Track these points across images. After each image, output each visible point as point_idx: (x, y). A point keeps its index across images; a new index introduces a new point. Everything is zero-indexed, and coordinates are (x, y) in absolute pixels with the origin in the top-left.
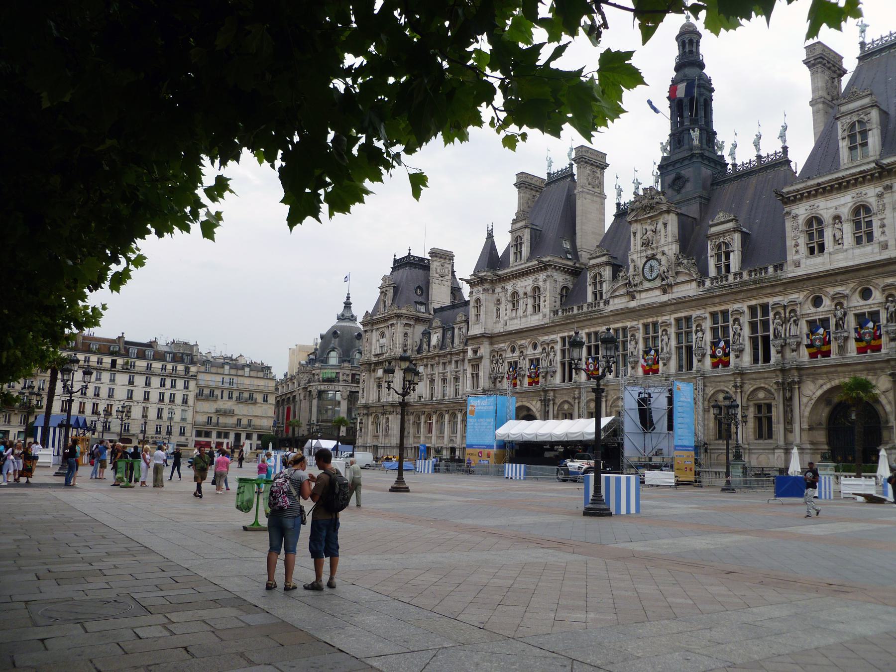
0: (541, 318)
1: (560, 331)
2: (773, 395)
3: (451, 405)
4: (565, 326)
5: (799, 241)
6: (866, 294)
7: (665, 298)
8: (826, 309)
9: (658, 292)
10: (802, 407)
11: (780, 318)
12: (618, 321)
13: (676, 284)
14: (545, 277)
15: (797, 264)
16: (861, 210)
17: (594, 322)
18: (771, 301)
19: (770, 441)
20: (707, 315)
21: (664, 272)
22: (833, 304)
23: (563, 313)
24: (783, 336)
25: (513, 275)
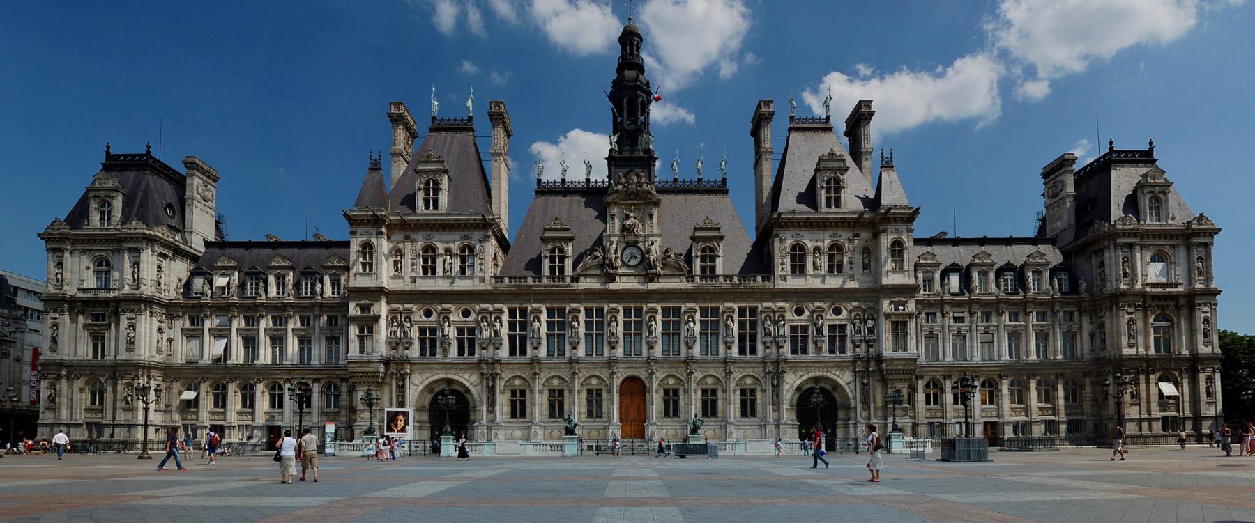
2: (760, 381)
5: (785, 260)
6: (837, 311)
7: (652, 286)
10: (785, 392)
11: (770, 320)
12: (592, 301)
13: (665, 275)
15: (784, 279)
16: (836, 248)
19: (755, 419)
20: (698, 309)
21: (654, 261)
23: (511, 282)
24: (772, 334)
25: (427, 225)
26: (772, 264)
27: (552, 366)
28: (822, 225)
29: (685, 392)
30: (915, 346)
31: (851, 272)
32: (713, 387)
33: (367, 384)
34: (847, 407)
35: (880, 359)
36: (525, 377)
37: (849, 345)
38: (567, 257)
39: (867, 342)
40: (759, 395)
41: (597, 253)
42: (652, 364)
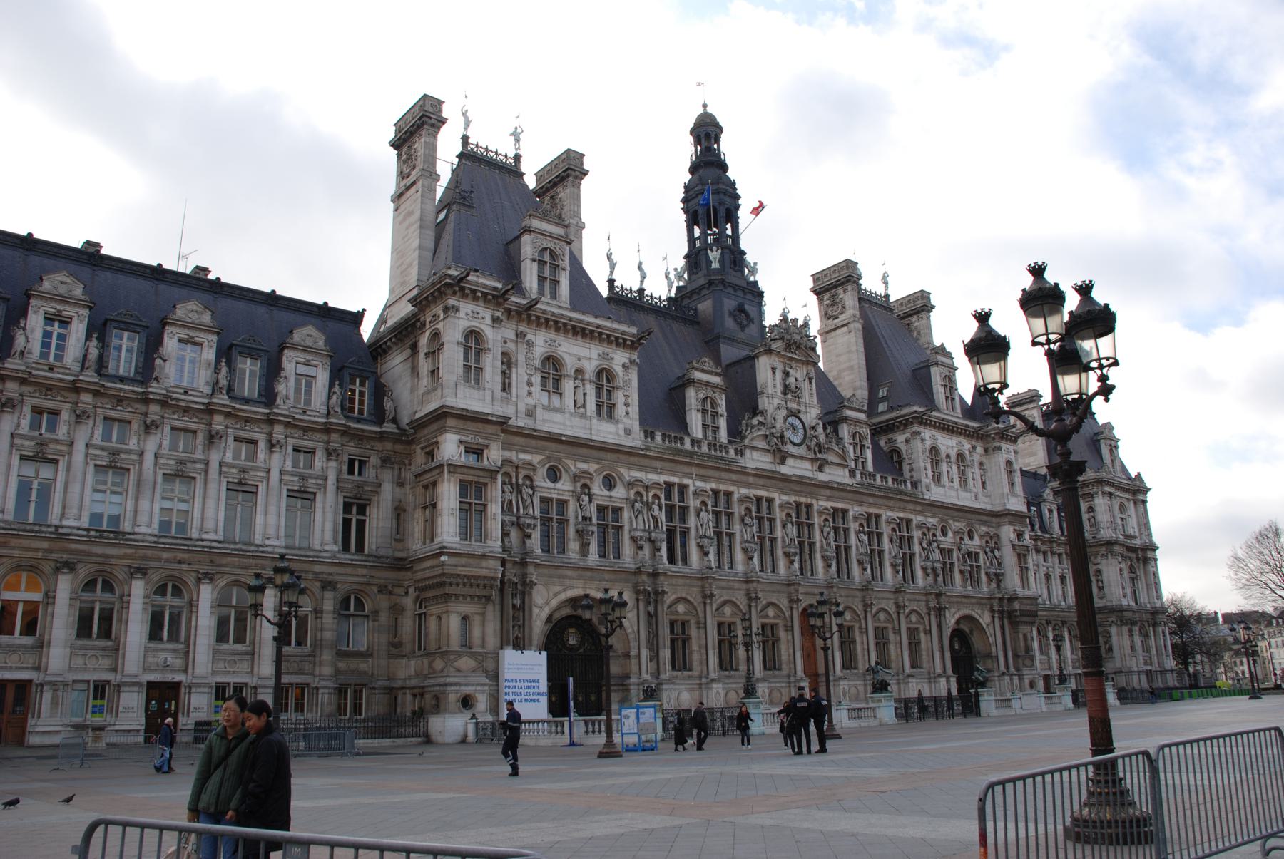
0: (622, 433)
1: (663, 471)
3: (165, 555)
4: (673, 465)
6: (971, 538)
7: (823, 477)
8: (952, 540)
9: (807, 465)
12: (763, 487)
14: (626, 360)
16: (960, 456)
17: (723, 475)
18: (918, 519)
22: (958, 538)
23: (664, 440)
25: (556, 322)
26: (906, 468)
27: (724, 584)
28: (949, 429)
29: (861, 632)
30: (1036, 587)
31: (974, 490)
32: (884, 625)
33: (469, 599)
34: (989, 656)
35: (1013, 598)
36: (692, 600)
37: (984, 578)
38: (722, 416)
39: (997, 575)
40: (923, 637)
41: (761, 419)
42: (835, 590)
